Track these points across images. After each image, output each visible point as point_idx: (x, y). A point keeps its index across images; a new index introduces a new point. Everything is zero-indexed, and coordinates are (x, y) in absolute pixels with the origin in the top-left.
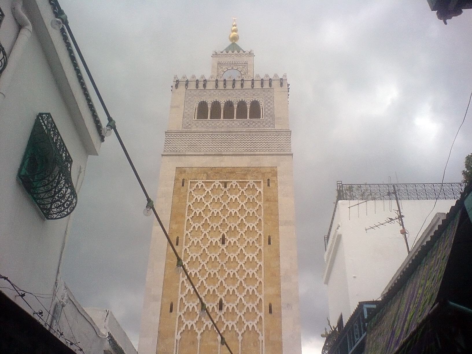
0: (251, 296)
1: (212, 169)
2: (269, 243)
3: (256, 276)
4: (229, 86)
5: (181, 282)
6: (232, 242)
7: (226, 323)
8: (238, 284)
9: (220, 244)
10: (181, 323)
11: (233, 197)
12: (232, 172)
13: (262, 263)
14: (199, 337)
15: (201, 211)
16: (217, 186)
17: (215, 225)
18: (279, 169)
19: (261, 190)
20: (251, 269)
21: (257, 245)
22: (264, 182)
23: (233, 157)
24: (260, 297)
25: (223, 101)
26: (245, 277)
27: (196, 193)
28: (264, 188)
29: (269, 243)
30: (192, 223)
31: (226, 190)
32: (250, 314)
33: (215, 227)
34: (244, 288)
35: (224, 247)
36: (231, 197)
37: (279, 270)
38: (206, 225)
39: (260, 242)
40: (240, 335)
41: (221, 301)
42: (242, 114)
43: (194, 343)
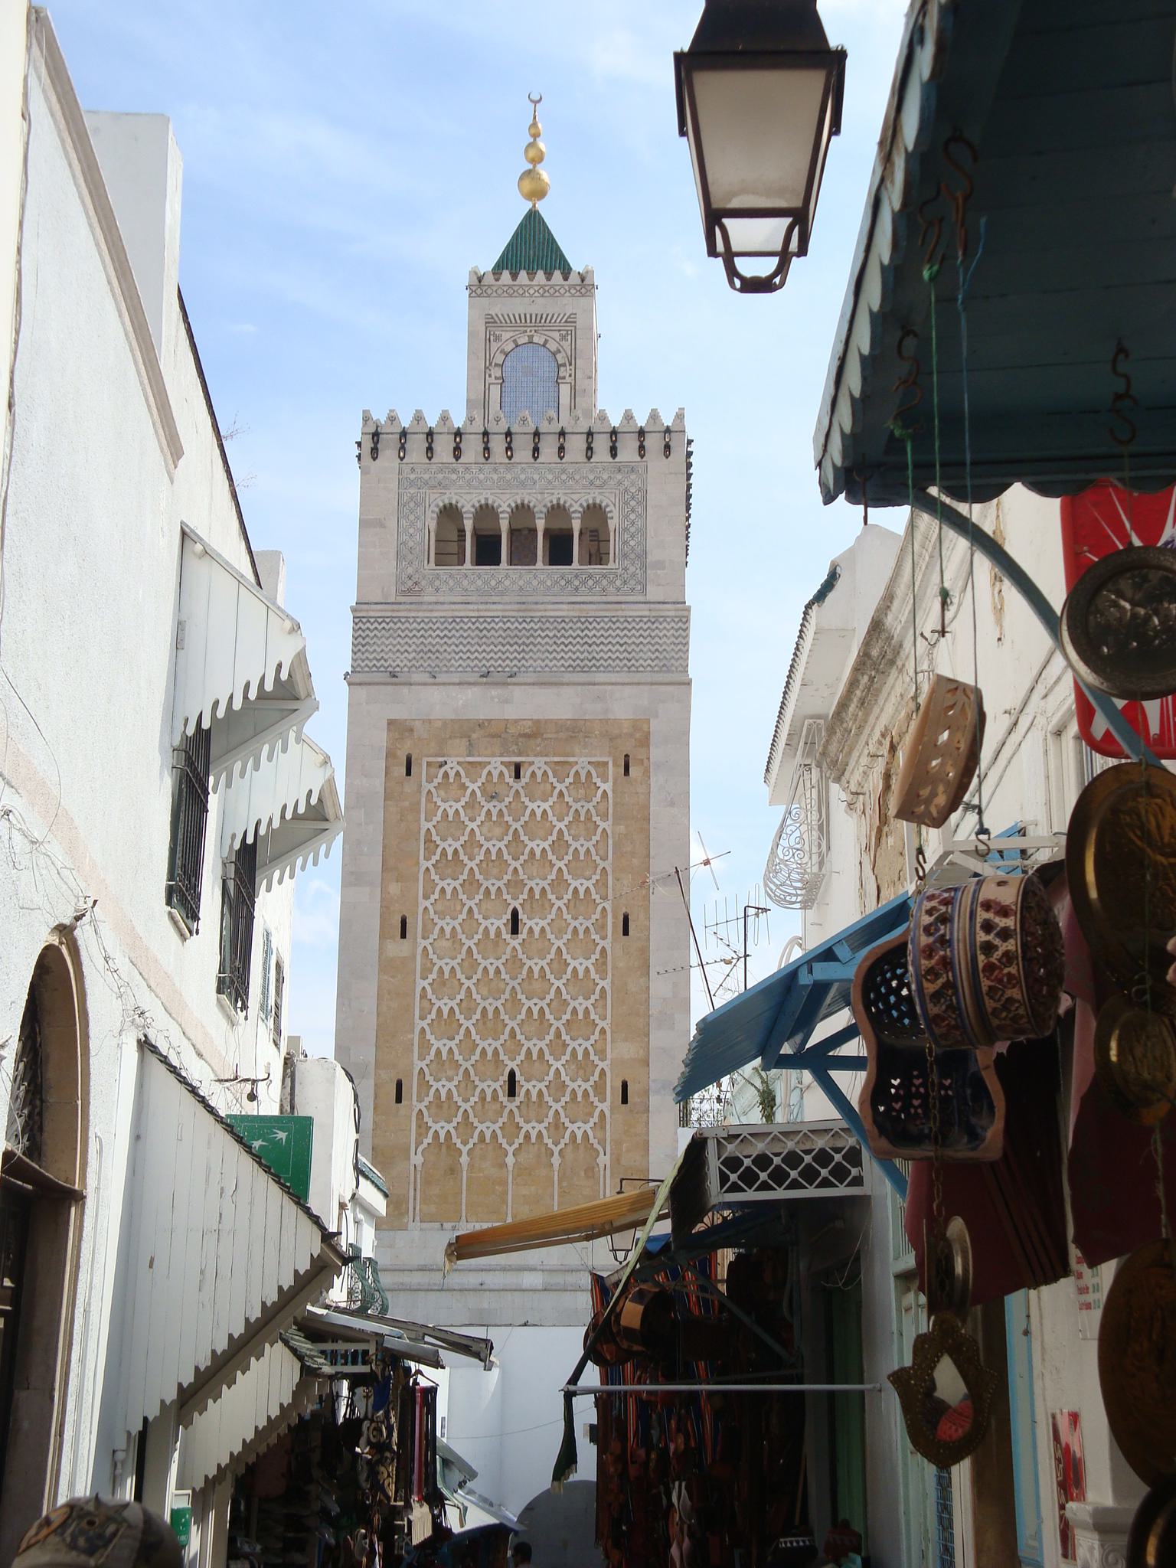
0: (582, 1066)
1: (481, 725)
2: (626, 932)
3: (593, 1016)
4: (523, 454)
5: (417, 1030)
6: (537, 930)
7: (526, 1127)
8: (551, 1036)
9: (506, 935)
10: (423, 1127)
11: (539, 807)
12: (534, 733)
13: (606, 984)
14: (464, 1159)
15: (457, 845)
16: (495, 774)
17: (492, 884)
18: (655, 726)
19: (607, 786)
20: (581, 999)
21: (597, 937)
22: (615, 764)
23: (536, 690)
24: (601, 1065)
25: (504, 504)
26: (568, 1016)
27: (442, 793)
28: (614, 783)
29: (626, 932)
30: (436, 878)
31: (517, 786)
32: (580, 1106)
33: (493, 890)
34: (565, 1045)
35: (515, 942)
36: (531, 806)
37: (647, 1000)
38: (471, 884)
39: (604, 926)
40: (556, 1154)
41: (512, 1075)
42: (560, 551)
43: (453, 1171)
